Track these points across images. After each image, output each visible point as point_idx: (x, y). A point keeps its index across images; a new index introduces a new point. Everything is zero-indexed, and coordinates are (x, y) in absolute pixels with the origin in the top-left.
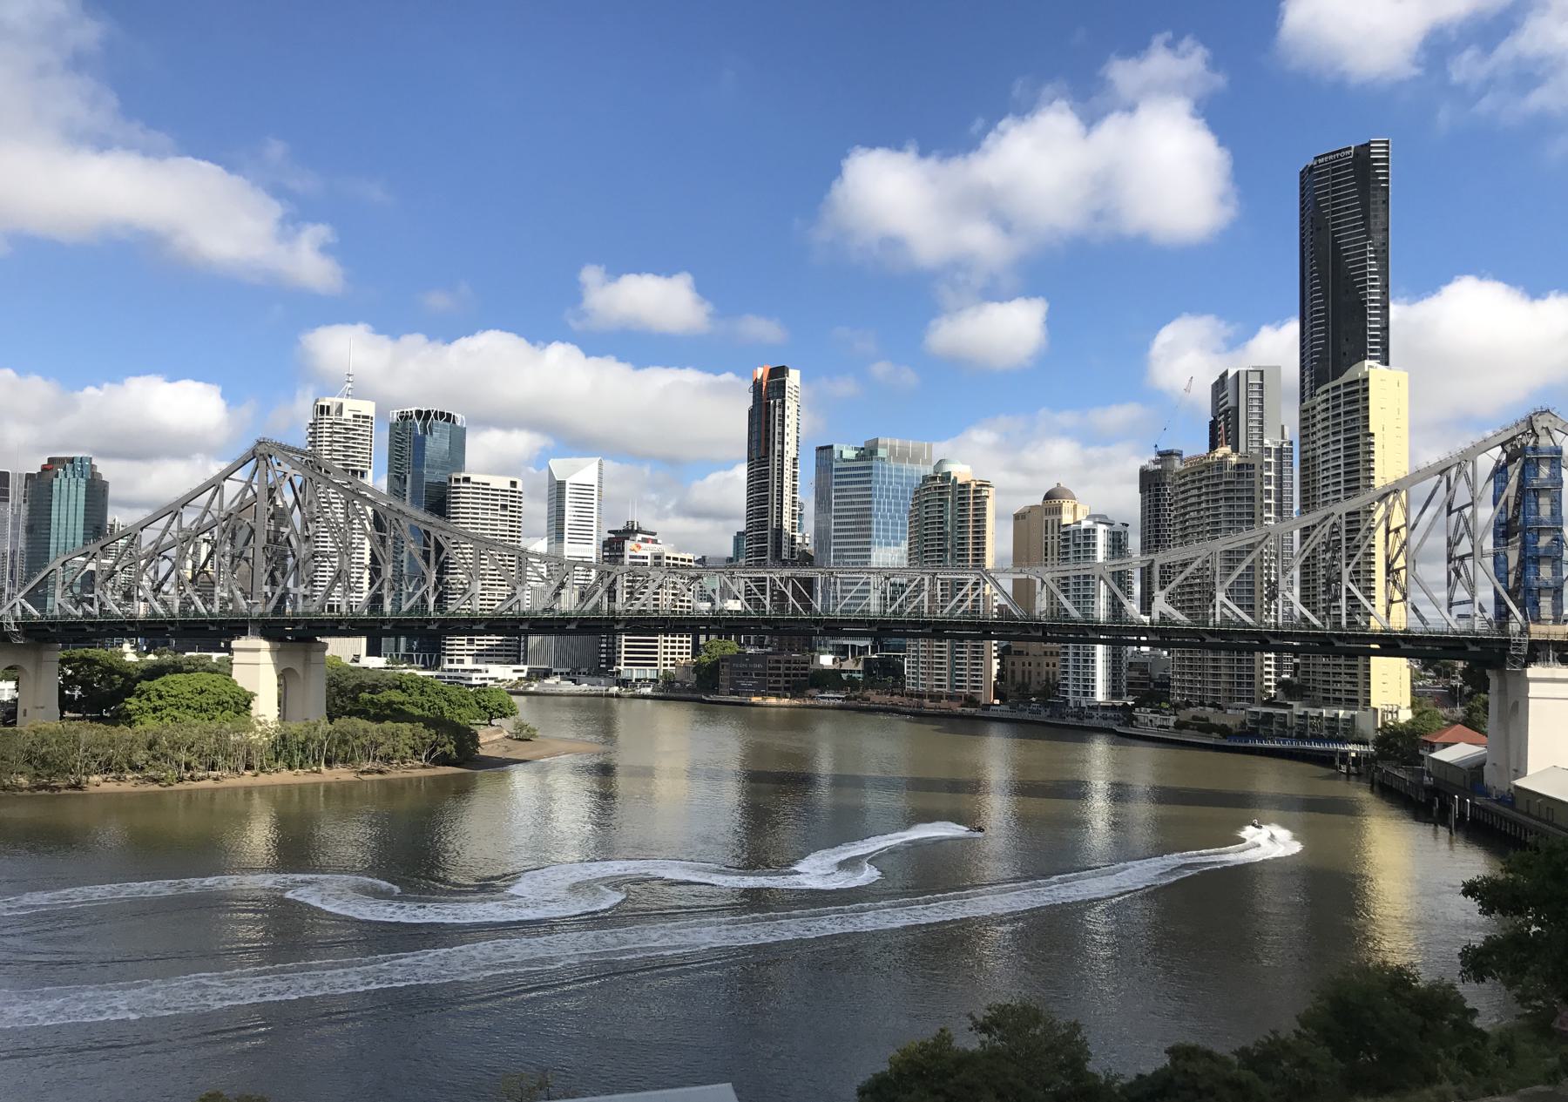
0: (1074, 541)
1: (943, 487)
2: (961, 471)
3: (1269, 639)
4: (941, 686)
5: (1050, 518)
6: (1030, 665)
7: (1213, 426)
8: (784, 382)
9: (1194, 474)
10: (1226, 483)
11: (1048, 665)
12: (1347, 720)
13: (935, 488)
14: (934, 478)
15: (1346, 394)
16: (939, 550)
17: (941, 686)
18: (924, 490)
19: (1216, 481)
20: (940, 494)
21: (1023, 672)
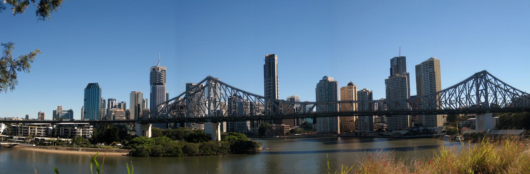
0: (361, 95)
1: (325, 83)
2: (330, 79)
3: (444, 112)
4: (327, 130)
5: (350, 90)
6: (346, 124)
7: (391, 69)
8: (274, 58)
9: (392, 80)
10: (400, 82)
11: (351, 124)
12: (433, 130)
13: (324, 83)
14: (323, 81)
15: (429, 64)
16: (325, 98)
17: (327, 130)
18: (320, 84)
19: (398, 81)
20: (325, 84)
21: (345, 126)
